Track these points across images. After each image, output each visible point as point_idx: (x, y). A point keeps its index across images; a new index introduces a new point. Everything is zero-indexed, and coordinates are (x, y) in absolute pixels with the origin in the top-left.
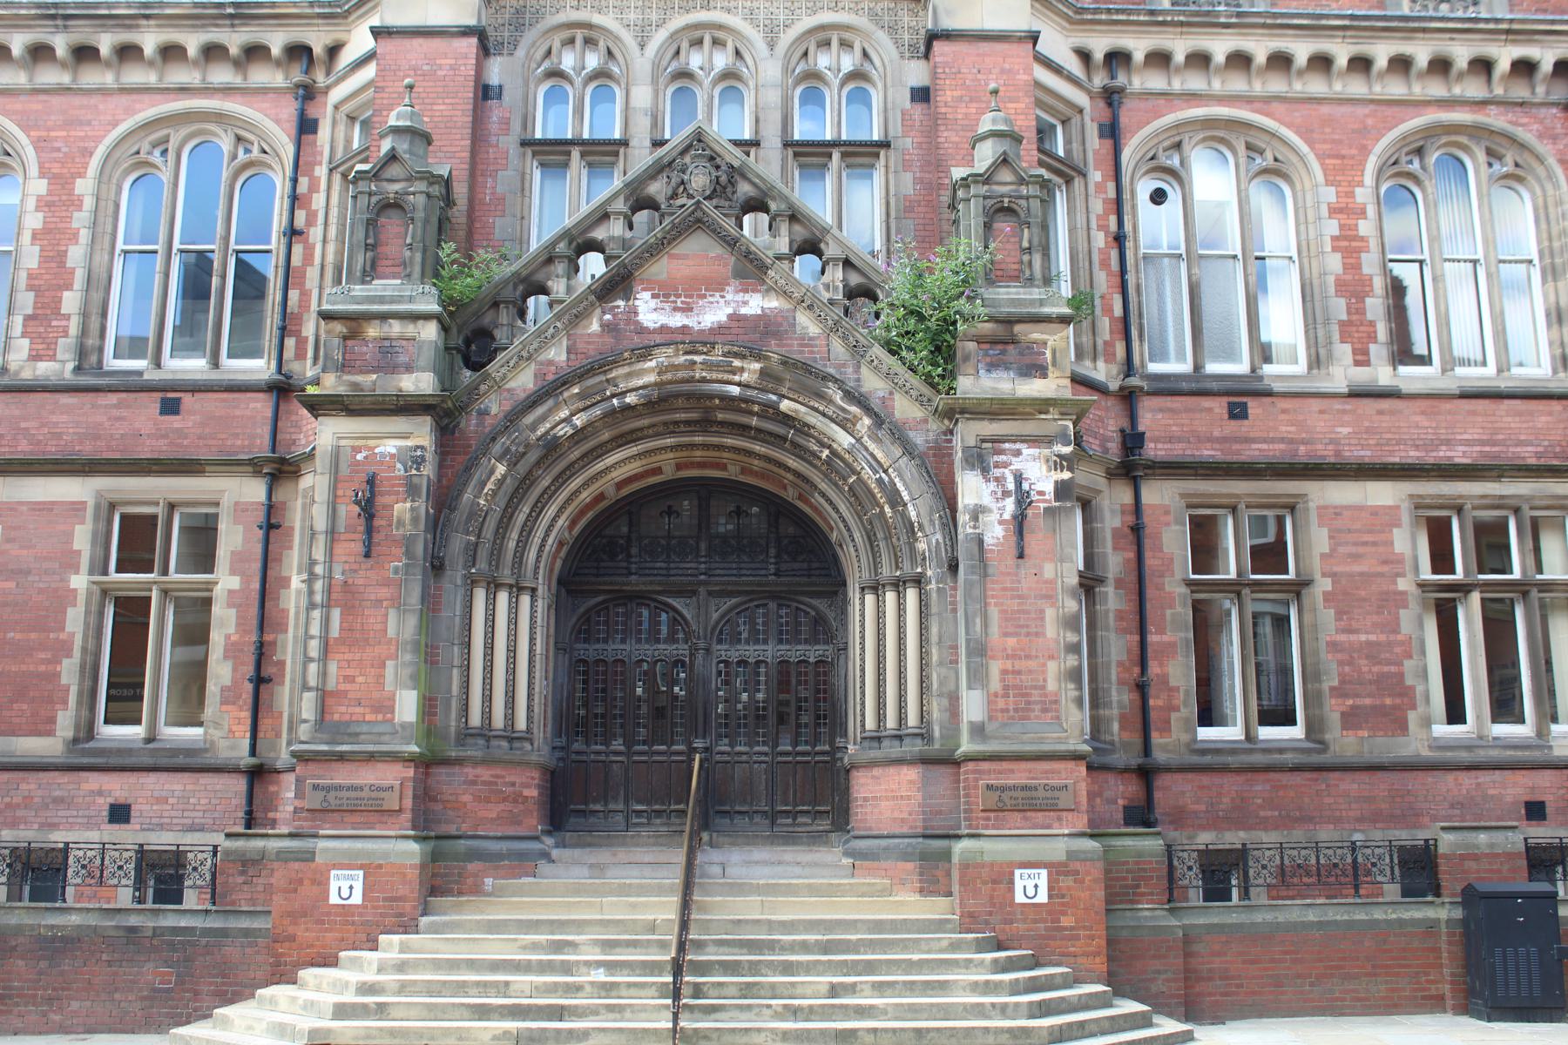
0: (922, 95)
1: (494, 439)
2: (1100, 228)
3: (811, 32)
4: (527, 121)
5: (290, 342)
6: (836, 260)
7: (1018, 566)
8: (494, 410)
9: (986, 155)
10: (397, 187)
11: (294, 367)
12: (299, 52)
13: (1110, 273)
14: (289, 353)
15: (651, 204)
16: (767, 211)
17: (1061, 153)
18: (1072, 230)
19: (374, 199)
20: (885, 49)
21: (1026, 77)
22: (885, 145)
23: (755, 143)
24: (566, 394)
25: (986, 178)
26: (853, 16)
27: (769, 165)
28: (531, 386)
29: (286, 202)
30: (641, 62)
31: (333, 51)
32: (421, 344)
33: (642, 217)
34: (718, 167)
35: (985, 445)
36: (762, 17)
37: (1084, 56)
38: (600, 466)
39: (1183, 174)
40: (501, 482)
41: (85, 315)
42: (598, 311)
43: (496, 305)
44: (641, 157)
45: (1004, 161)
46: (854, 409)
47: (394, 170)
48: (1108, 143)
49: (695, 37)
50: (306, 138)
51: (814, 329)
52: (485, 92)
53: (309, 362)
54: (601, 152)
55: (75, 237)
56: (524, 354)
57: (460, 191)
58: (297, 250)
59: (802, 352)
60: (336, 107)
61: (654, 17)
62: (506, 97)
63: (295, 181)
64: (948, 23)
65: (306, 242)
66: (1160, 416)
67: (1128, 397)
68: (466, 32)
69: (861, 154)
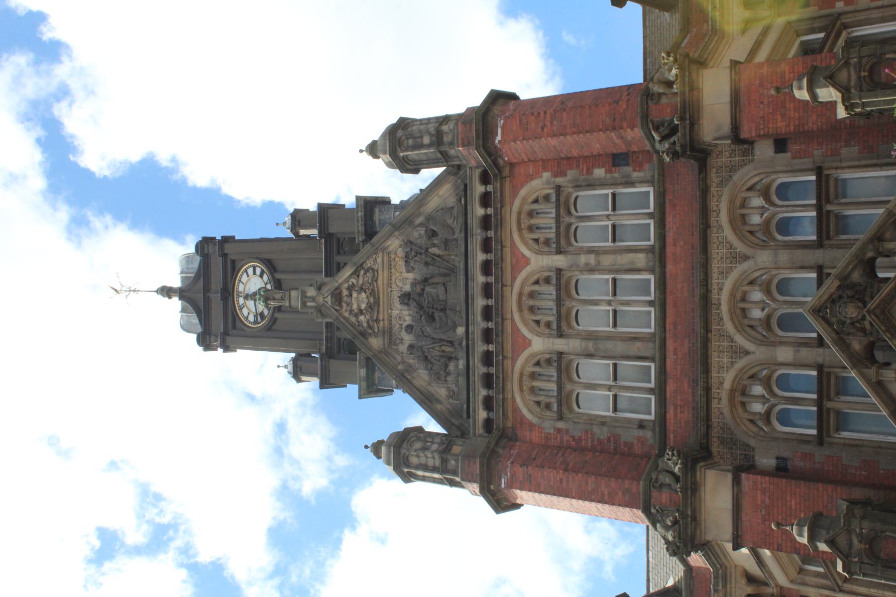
0: (781, 145)
3: (735, 230)
4: (803, 440)
9: (828, 94)
10: (855, 540)
15: (870, 348)
16: (873, 259)
18: (884, 20)
19: (866, 560)
20: (746, 175)
21: (765, 68)
22: (819, 171)
23: (820, 269)
25: (845, 91)
26: (723, 198)
27: (839, 259)
30: (760, 353)
31: (751, 579)
33: (879, 356)
34: (840, 297)
36: (724, 265)
44: (834, 354)
45: (832, 80)
47: (842, 541)
49: (740, 314)
52: (782, 470)
54: (827, 384)
57: (858, 493)
60: (792, 582)
61: (726, 344)
62: (786, 454)
64: (726, 128)
68: (737, 482)
69: (826, 191)
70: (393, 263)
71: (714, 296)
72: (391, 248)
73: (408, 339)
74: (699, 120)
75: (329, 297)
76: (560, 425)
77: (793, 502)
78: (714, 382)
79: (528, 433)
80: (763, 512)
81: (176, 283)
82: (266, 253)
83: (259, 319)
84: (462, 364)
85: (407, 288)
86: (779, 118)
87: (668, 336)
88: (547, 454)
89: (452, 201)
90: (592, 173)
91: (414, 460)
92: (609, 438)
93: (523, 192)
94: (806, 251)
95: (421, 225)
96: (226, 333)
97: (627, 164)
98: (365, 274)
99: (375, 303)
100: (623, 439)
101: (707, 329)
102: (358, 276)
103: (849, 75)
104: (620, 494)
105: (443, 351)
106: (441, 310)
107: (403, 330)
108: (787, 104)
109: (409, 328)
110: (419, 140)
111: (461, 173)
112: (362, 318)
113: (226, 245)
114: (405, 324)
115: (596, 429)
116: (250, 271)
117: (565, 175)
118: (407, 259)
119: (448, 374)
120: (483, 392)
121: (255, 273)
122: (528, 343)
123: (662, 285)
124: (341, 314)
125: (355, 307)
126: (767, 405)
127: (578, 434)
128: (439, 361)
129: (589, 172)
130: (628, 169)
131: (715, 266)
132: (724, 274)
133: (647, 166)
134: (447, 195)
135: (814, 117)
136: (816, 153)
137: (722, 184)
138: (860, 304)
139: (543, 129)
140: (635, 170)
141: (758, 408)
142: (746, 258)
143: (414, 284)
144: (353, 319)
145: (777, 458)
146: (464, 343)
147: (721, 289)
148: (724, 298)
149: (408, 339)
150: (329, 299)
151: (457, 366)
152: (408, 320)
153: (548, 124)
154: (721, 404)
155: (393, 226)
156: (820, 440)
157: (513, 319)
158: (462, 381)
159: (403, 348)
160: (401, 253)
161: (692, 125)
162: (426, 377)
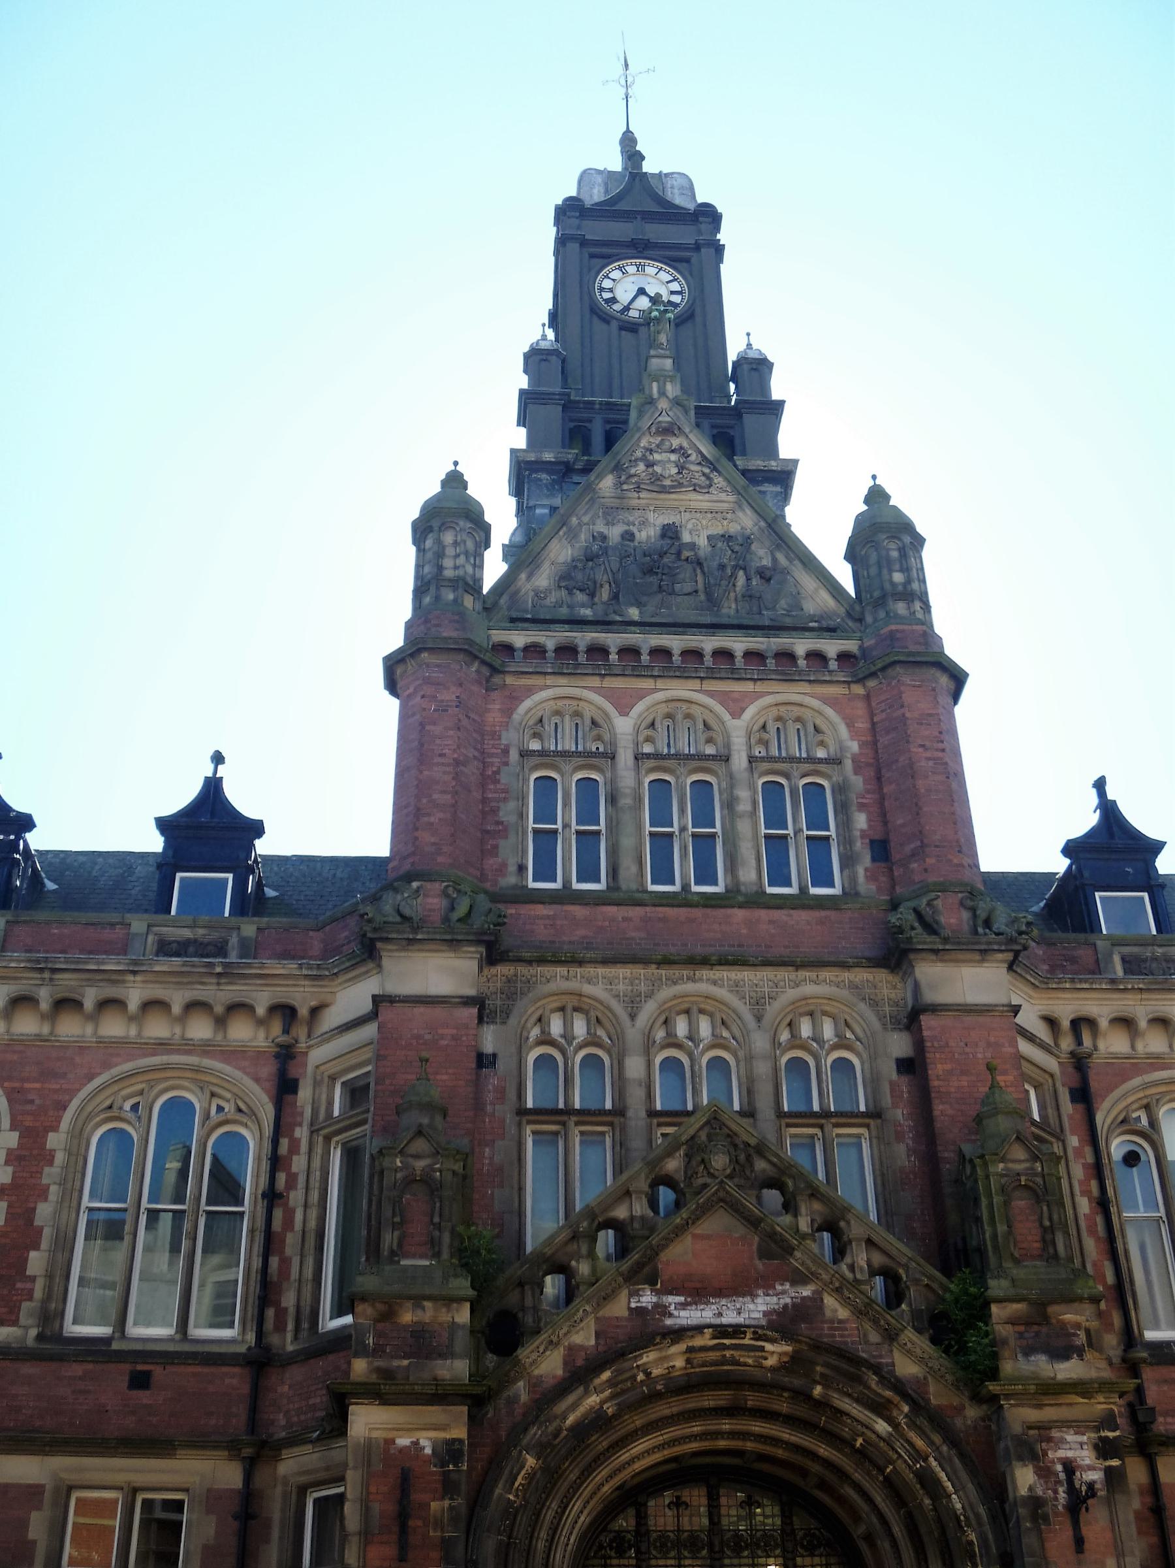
0: (906, 1066)
1: (526, 1430)
2: (1083, 1193)
5: (270, 1313)
6: (859, 1240)
7: (1079, 1563)
8: (524, 1397)
11: (274, 1340)
12: (286, 1012)
13: (1098, 1239)
14: (269, 1324)
17: (1036, 1117)
19: (399, 1175)
21: (1010, 1050)
24: (597, 1381)
26: (834, 989)
28: (560, 1372)
29: (265, 1166)
32: (453, 1326)
34: (735, 1146)
35: (1032, 1432)
36: (747, 989)
37: (1051, 1022)
38: (625, 1456)
39: (1155, 1137)
40: (531, 1477)
41: (50, 1276)
42: (625, 1292)
43: (521, 1285)
46: (888, 1393)
48: (1080, 1107)
50: (289, 1098)
51: (843, 1313)
53: (289, 1336)
55: (43, 1194)
56: (555, 1339)
58: (278, 1214)
59: (834, 1336)
61: (643, 988)
62: (501, 1064)
63: (275, 1142)
65: (286, 1204)
66: (1165, 1388)
67: (1132, 1368)
68: (467, 1001)
70: (719, 516)
71: (705, 973)
72: (740, 514)
73: (614, 533)
74: (942, 961)
75: (669, 419)
76: (514, 755)
77: (445, 1077)
78: (590, 970)
79: (498, 707)
80: (427, 1037)
81: (648, 167)
82: (701, 313)
83: (606, 295)
84: (587, 612)
85: (686, 538)
86: (948, 1067)
87: (648, 909)
88: (475, 735)
89: (810, 607)
90: (860, 810)
91: (448, 538)
92: (499, 823)
93: (829, 712)
94: (771, 1098)
95: (775, 560)
96: (584, 243)
97: (874, 859)
98: (704, 474)
99: (664, 487)
100: (502, 843)
101: (666, 962)
102: (699, 464)
103: (1020, 1161)
104: (433, 840)
105: (601, 586)
106: (660, 587)
107: (626, 528)
108: (965, 1078)
109: (628, 536)
110: (897, 567)
111: (850, 624)
112: (641, 467)
113: (712, 250)
114: (634, 530)
115: (512, 805)
116: (675, 286)
117: (856, 773)
118: (727, 538)
119: (570, 592)
120: (550, 645)
121: (672, 293)
122: (624, 713)
123: (709, 901)
124: (644, 434)
125: (657, 457)
126: (563, 1041)
127: (504, 779)
128: (588, 580)
129: (862, 807)
130: (867, 860)
131: (746, 975)
132: (736, 987)
133: (873, 887)
134: (818, 600)
135: (950, 1112)
136: (899, 1112)
137: (853, 987)
138: (728, 1171)
139: (923, 746)
140: (866, 870)
141: (556, 1027)
142: (759, 1019)
143: (693, 546)
144: (639, 454)
145: (494, 1055)
146: (618, 618)
147: (715, 983)
148: (703, 987)
149: (614, 533)
150: (665, 418)
151: (583, 606)
152: (642, 536)
153: (928, 754)
154: (559, 979)
155: (774, 521)
156: (522, 1112)
157: (656, 690)
158: (564, 612)
159: (600, 527)
160: (734, 529)
161: (936, 952)
162: (561, 559)
